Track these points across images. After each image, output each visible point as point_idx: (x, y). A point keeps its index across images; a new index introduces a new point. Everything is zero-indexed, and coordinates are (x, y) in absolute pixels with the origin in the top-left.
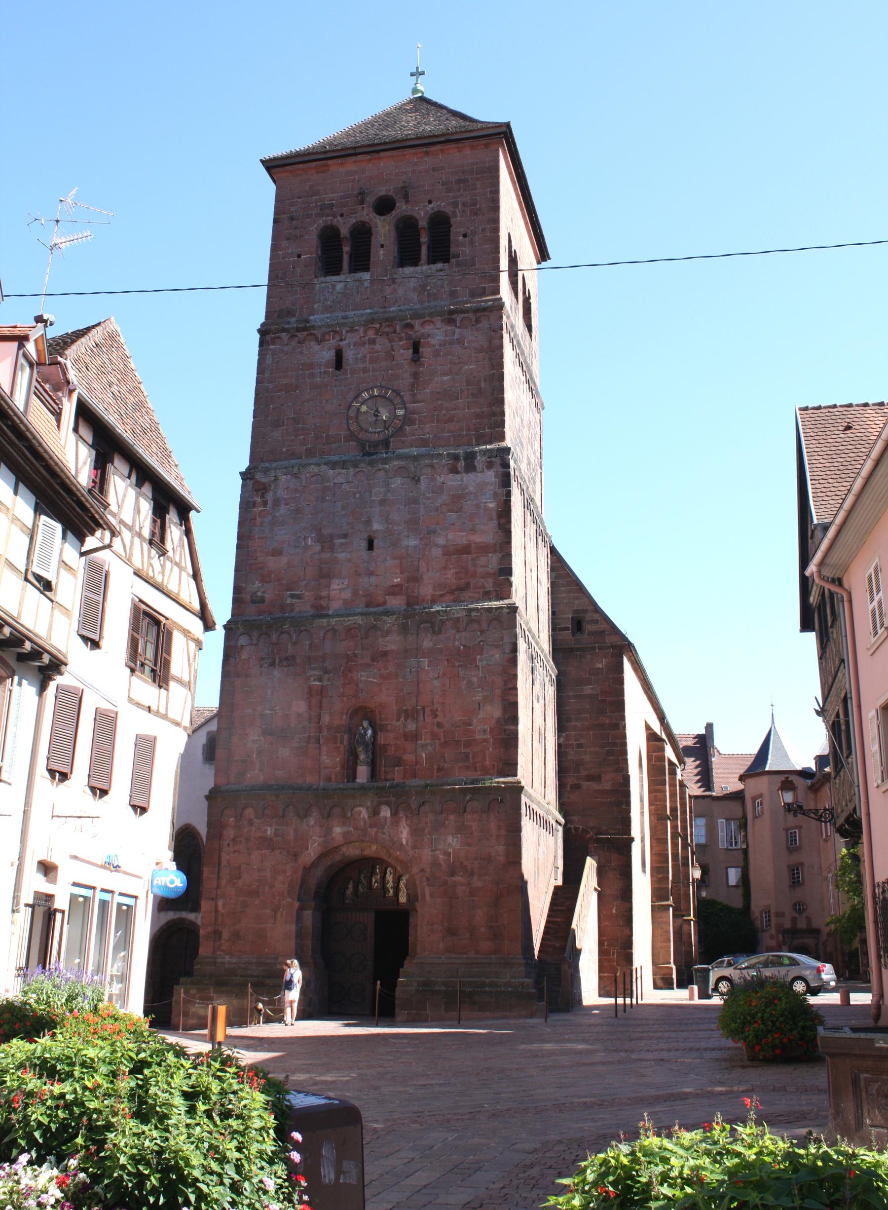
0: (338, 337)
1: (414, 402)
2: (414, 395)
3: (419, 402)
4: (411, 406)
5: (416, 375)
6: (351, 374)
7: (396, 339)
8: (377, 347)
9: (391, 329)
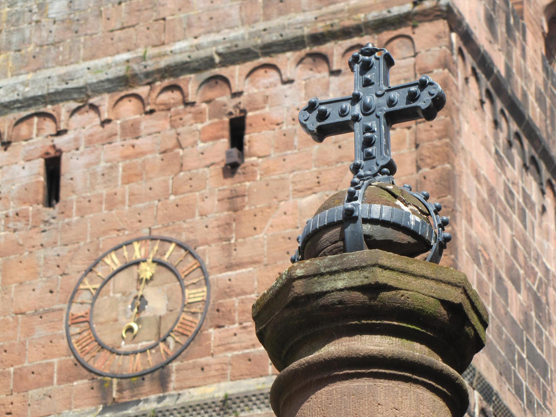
0: (49, 127)
1: (230, 267)
2: (228, 249)
3: (240, 265)
4: (219, 277)
5: (234, 201)
6: (82, 212)
7: (188, 117)
8: (144, 143)
9: (176, 95)
